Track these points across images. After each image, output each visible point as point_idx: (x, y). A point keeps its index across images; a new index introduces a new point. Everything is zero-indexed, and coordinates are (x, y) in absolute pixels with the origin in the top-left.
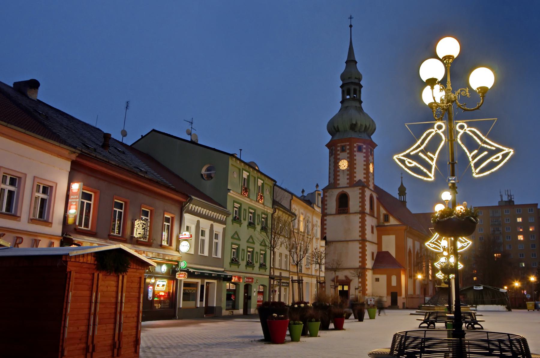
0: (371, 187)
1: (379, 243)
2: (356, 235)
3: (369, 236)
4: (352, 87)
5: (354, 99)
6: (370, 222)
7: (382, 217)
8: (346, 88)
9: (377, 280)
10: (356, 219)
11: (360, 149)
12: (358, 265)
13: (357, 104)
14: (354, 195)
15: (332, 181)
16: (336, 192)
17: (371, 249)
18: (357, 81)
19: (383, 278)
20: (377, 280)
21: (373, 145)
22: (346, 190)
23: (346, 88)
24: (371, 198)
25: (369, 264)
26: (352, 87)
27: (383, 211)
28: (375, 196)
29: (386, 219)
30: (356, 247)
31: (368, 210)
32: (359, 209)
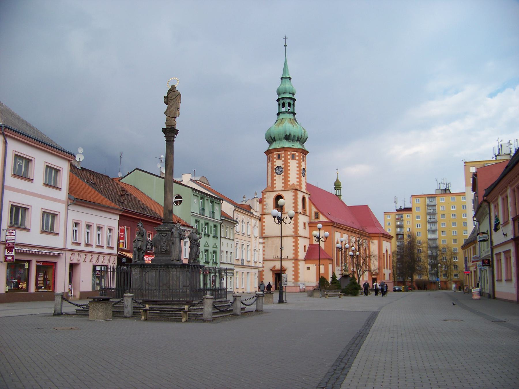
0: (304, 190)
3: (302, 231)
5: (288, 112)
6: (302, 219)
7: (313, 215)
8: (281, 102)
11: (293, 157)
13: (291, 116)
15: (270, 184)
16: (274, 195)
17: (303, 243)
22: (282, 193)
23: (281, 102)
24: (304, 199)
27: (314, 210)
28: (307, 197)
29: (317, 216)
31: (300, 209)
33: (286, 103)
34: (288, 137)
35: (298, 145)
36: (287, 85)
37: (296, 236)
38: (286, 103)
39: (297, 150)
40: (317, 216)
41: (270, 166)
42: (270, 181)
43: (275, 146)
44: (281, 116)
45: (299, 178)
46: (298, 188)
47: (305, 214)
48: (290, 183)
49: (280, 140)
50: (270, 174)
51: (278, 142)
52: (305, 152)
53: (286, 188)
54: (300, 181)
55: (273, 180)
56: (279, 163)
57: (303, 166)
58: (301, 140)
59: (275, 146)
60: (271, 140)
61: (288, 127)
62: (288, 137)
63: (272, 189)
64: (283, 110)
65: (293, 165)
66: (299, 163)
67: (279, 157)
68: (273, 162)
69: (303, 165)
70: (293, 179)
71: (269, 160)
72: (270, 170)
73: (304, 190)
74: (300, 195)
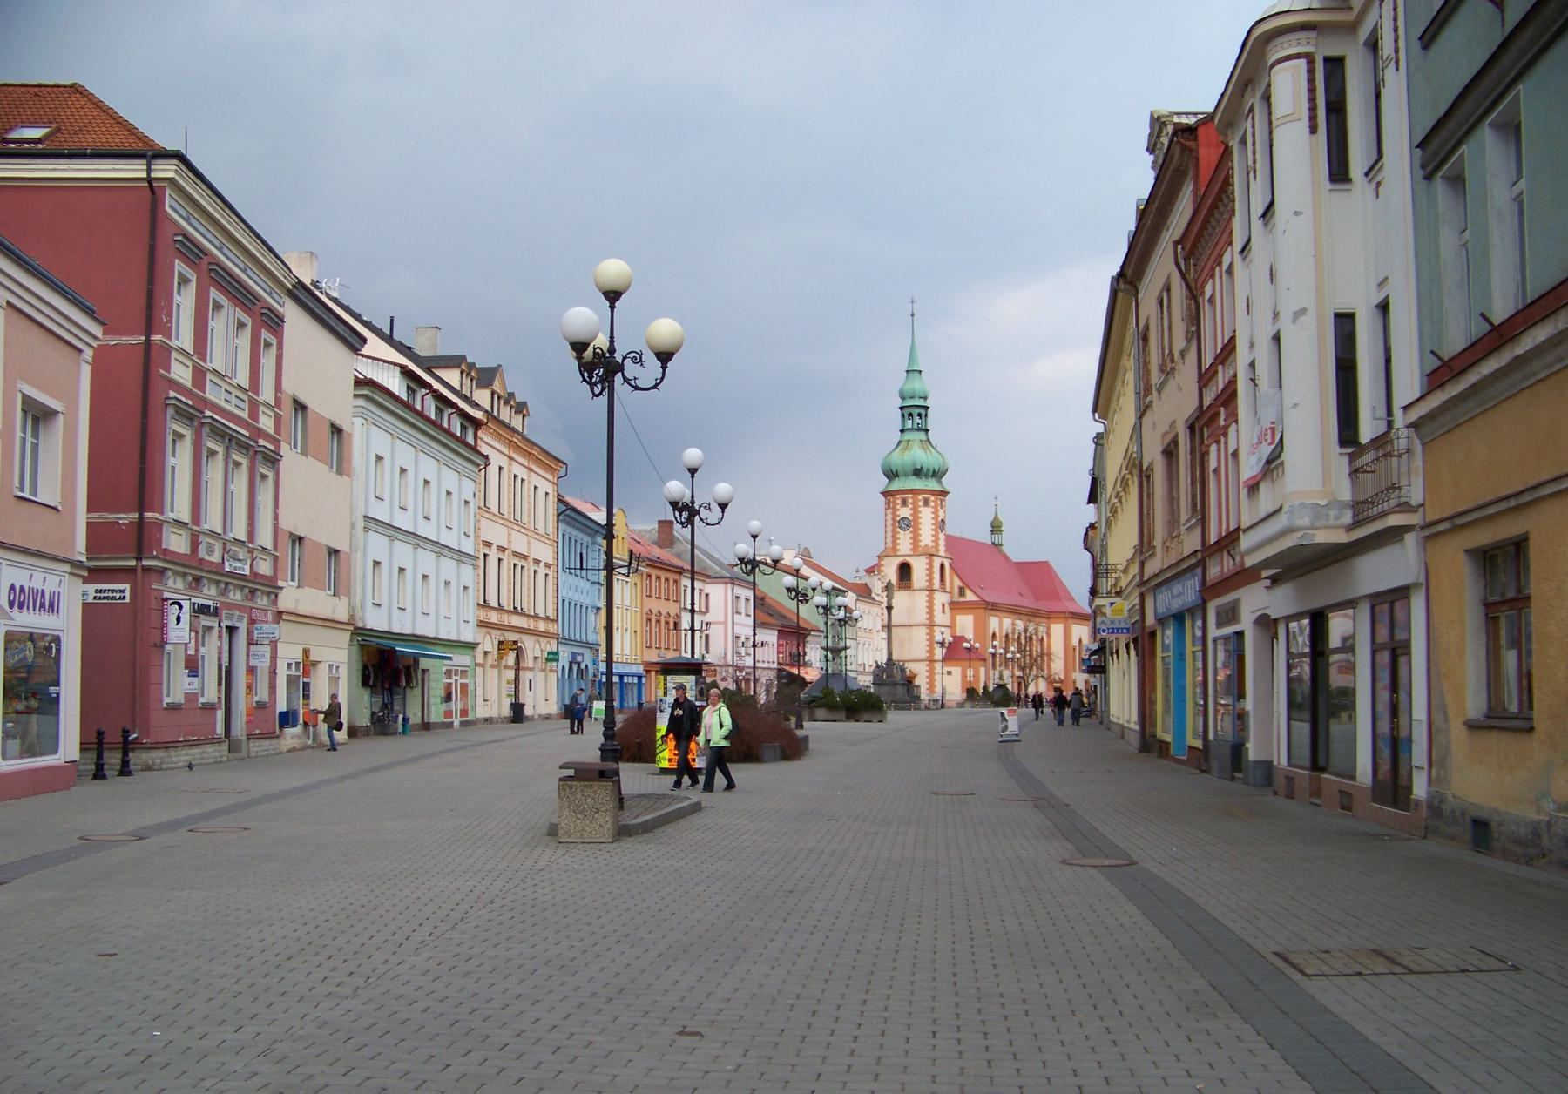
0: (942, 553)
1: (952, 626)
2: (922, 617)
3: (941, 618)
4: (916, 411)
5: (919, 430)
6: (941, 598)
8: (907, 412)
9: (949, 673)
10: (922, 598)
11: (926, 503)
12: (925, 655)
13: (922, 436)
14: (919, 567)
15: (890, 544)
16: (897, 561)
18: (921, 403)
19: (957, 671)
20: (949, 673)
21: (944, 493)
22: (908, 559)
23: (907, 412)
24: (942, 566)
25: (939, 653)
26: (916, 411)
27: (958, 583)
29: (962, 592)
30: (924, 631)
32: (925, 584)
33: (914, 413)
34: (918, 472)
35: (932, 484)
36: (916, 385)
37: (931, 625)
38: (914, 413)
39: (933, 492)
40: (962, 592)
41: (890, 516)
42: (889, 540)
43: (897, 485)
44: (908, 436)
45: (936, 536)
46: (933, 551)
47: (943, 590)
48: (922, 544)
49: (906, 475)
50: (890, 528)
51: (902, 479)
52: (944, 493)
53: (916, 550)
54: (936, 541)
55: (895, 538)
56: (904, 512)
57: (941, 515)
58: (937, 474)
59: (897, 485)
60: (891, 474)
61: (918, 455)
62: (918, 472)
63: (892, 551)
64: (909, 424)
65: (926, 515)
66: (936, 513)
67: (904, 503)
68: (895, 510)
69: (941, 515)
70: (926, 538)
71: (888, 504)
72: (890, 522)
73: (942, 553)
74: (937, 562)
